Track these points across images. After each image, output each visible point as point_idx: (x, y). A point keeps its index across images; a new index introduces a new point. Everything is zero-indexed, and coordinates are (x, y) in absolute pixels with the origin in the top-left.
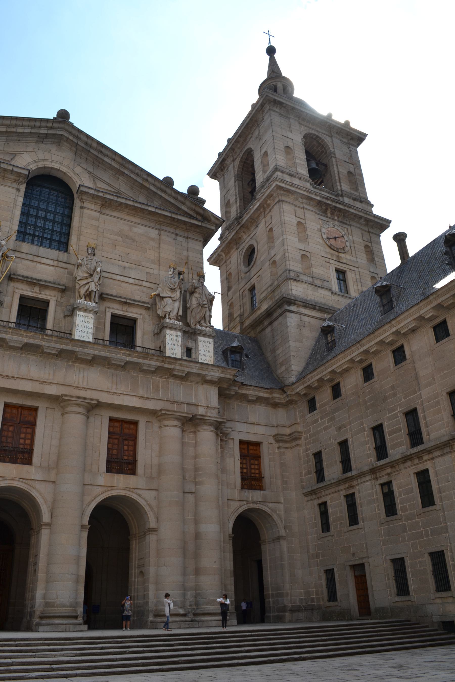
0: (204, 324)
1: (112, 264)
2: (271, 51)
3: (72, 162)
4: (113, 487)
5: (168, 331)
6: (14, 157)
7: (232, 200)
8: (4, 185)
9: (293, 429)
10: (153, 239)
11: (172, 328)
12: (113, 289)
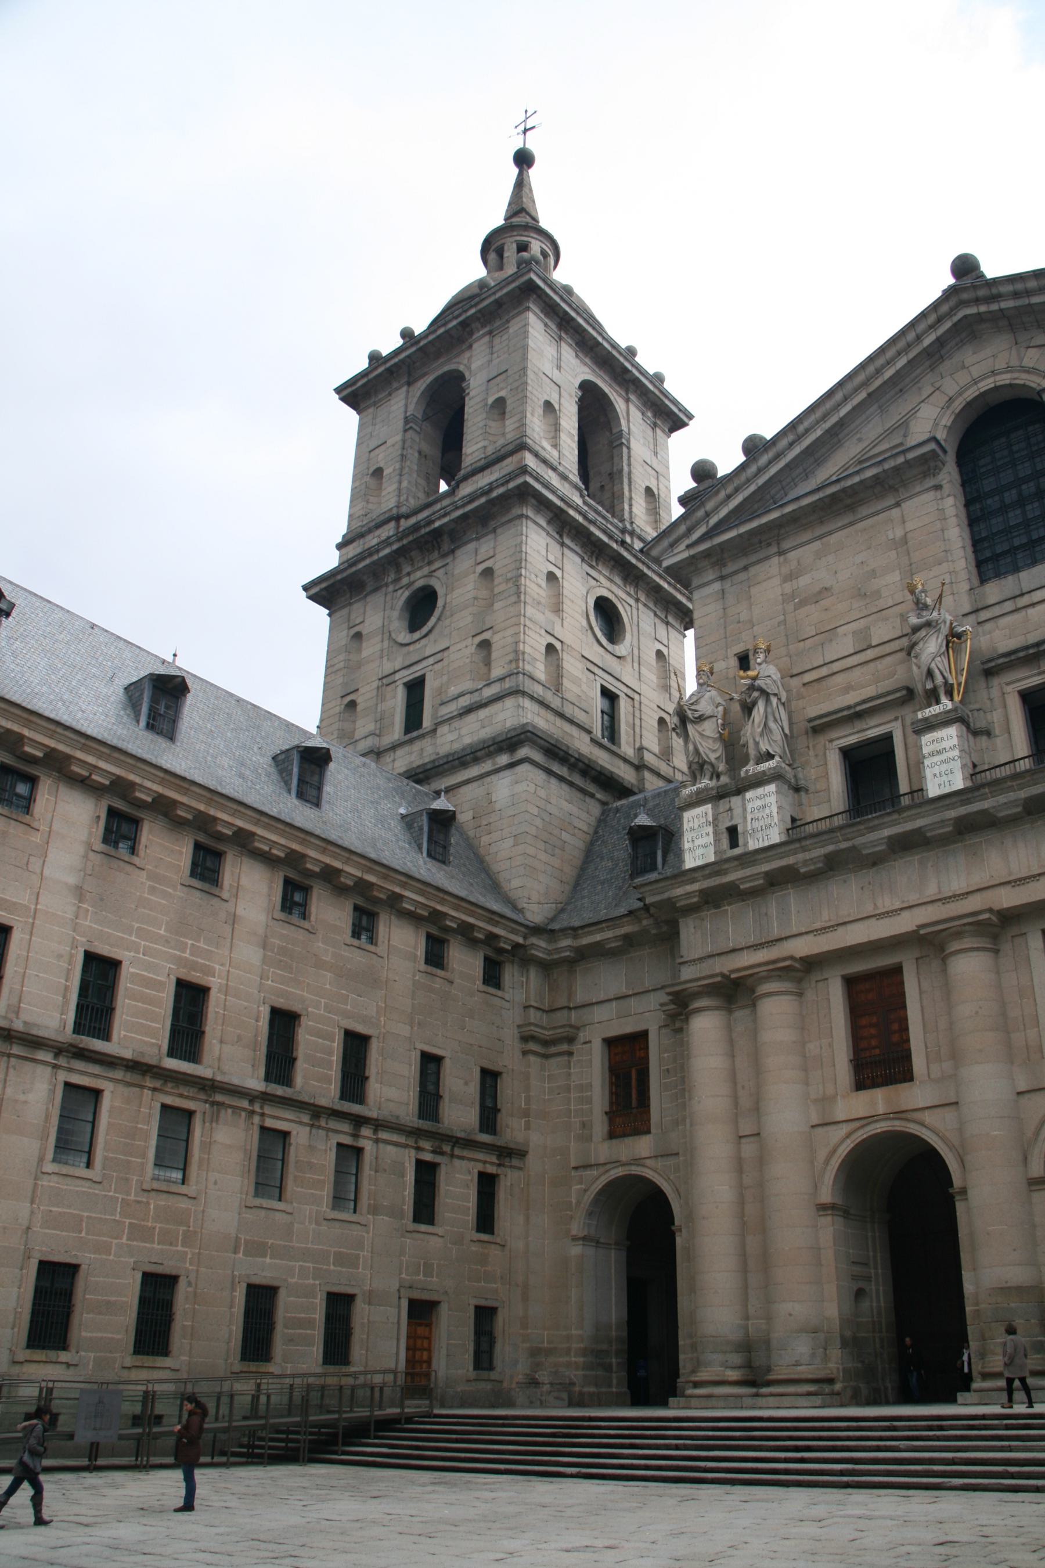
3: (1014, 352)
6: (907, 427)
8: (910, 497)
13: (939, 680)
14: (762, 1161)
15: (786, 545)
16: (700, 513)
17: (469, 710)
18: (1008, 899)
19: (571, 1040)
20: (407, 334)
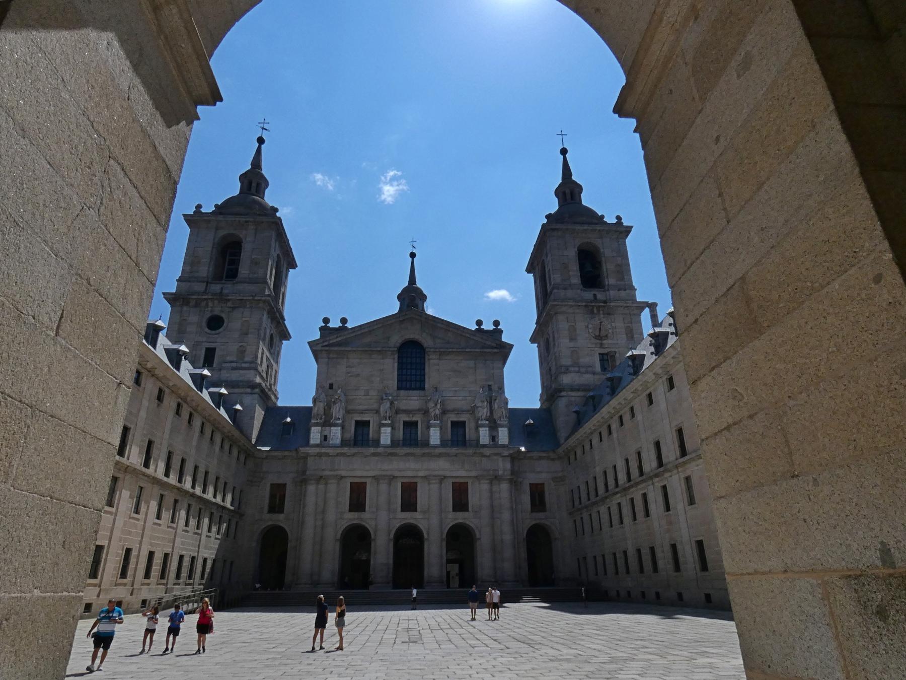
2: (564, 152)
4: (456, 519)
9: (560, 474)
11: (483, 426)
12: (449, 407)
14: (323, 527)
17: (234, 369)
18: (397, 474)
20: (216, 206)
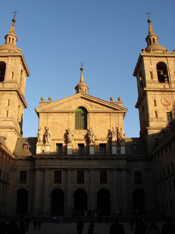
0: (123, 143)
1: (98, 130)
5: (113, 147)
7: (139, 87)
10: (108, 119)
11: (114, 146)
13: (71, 141)
15: (53, 115)
16: (44, 107)
17: (4, 121)
19: (15, 170)
